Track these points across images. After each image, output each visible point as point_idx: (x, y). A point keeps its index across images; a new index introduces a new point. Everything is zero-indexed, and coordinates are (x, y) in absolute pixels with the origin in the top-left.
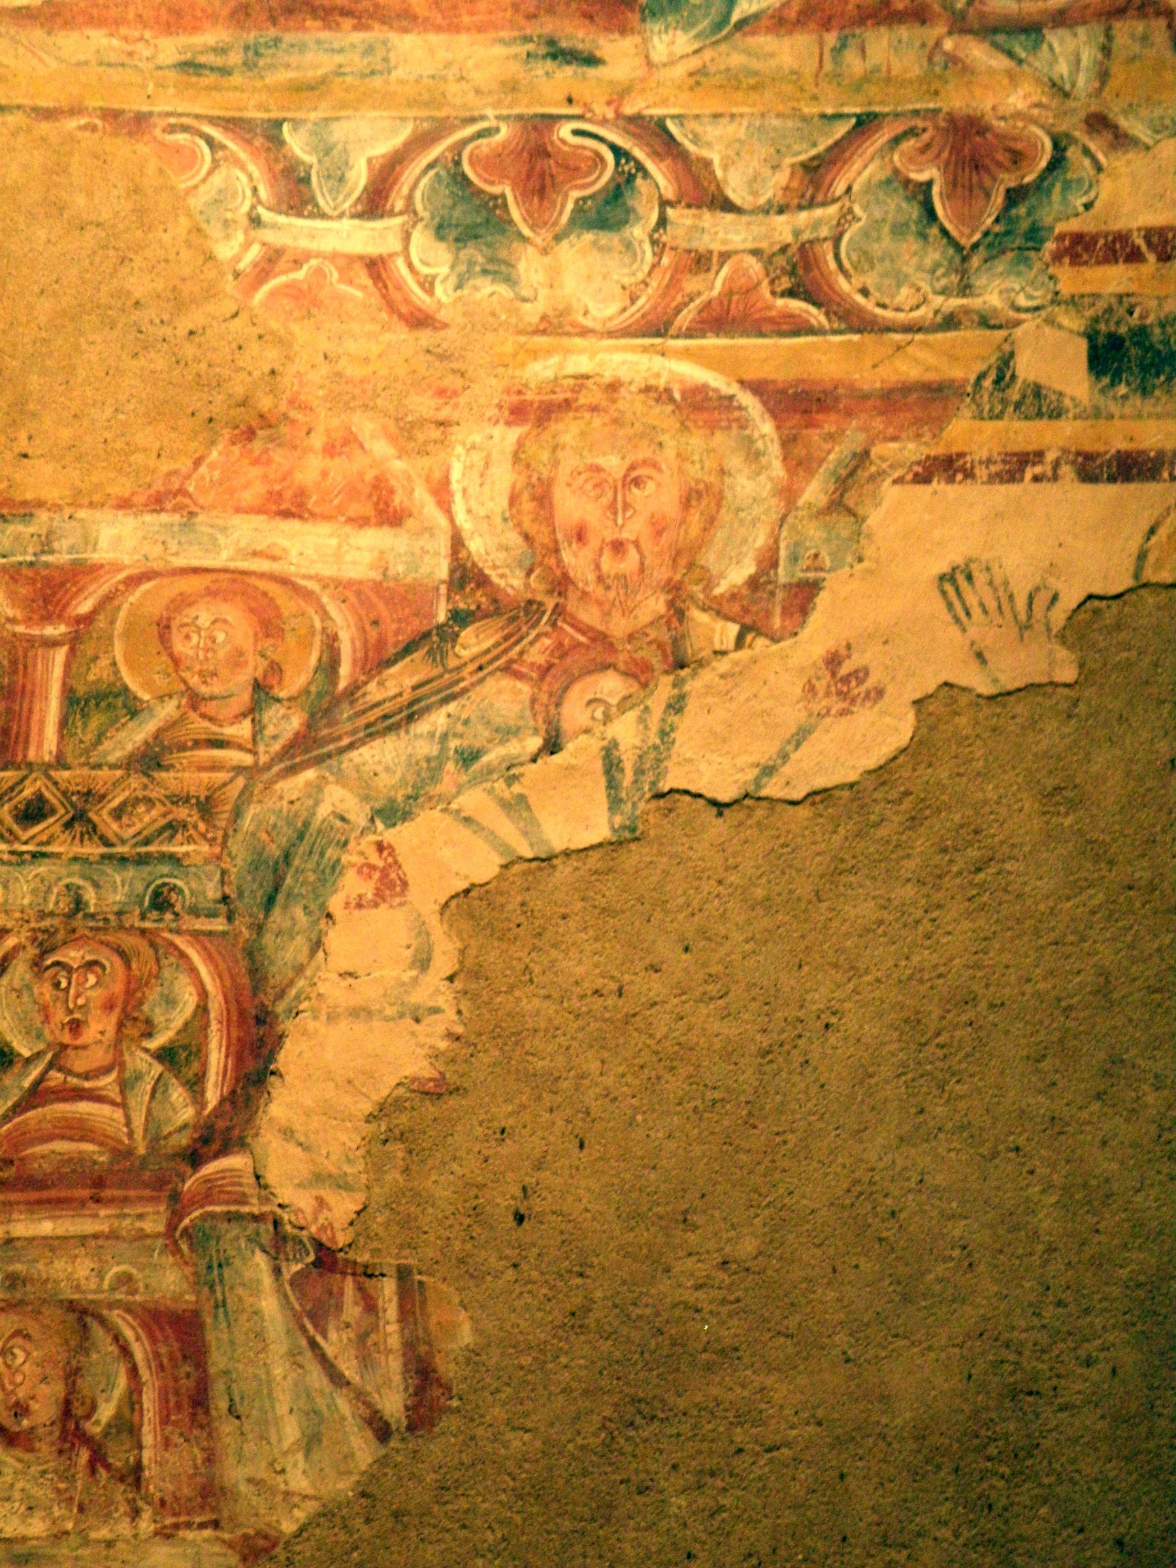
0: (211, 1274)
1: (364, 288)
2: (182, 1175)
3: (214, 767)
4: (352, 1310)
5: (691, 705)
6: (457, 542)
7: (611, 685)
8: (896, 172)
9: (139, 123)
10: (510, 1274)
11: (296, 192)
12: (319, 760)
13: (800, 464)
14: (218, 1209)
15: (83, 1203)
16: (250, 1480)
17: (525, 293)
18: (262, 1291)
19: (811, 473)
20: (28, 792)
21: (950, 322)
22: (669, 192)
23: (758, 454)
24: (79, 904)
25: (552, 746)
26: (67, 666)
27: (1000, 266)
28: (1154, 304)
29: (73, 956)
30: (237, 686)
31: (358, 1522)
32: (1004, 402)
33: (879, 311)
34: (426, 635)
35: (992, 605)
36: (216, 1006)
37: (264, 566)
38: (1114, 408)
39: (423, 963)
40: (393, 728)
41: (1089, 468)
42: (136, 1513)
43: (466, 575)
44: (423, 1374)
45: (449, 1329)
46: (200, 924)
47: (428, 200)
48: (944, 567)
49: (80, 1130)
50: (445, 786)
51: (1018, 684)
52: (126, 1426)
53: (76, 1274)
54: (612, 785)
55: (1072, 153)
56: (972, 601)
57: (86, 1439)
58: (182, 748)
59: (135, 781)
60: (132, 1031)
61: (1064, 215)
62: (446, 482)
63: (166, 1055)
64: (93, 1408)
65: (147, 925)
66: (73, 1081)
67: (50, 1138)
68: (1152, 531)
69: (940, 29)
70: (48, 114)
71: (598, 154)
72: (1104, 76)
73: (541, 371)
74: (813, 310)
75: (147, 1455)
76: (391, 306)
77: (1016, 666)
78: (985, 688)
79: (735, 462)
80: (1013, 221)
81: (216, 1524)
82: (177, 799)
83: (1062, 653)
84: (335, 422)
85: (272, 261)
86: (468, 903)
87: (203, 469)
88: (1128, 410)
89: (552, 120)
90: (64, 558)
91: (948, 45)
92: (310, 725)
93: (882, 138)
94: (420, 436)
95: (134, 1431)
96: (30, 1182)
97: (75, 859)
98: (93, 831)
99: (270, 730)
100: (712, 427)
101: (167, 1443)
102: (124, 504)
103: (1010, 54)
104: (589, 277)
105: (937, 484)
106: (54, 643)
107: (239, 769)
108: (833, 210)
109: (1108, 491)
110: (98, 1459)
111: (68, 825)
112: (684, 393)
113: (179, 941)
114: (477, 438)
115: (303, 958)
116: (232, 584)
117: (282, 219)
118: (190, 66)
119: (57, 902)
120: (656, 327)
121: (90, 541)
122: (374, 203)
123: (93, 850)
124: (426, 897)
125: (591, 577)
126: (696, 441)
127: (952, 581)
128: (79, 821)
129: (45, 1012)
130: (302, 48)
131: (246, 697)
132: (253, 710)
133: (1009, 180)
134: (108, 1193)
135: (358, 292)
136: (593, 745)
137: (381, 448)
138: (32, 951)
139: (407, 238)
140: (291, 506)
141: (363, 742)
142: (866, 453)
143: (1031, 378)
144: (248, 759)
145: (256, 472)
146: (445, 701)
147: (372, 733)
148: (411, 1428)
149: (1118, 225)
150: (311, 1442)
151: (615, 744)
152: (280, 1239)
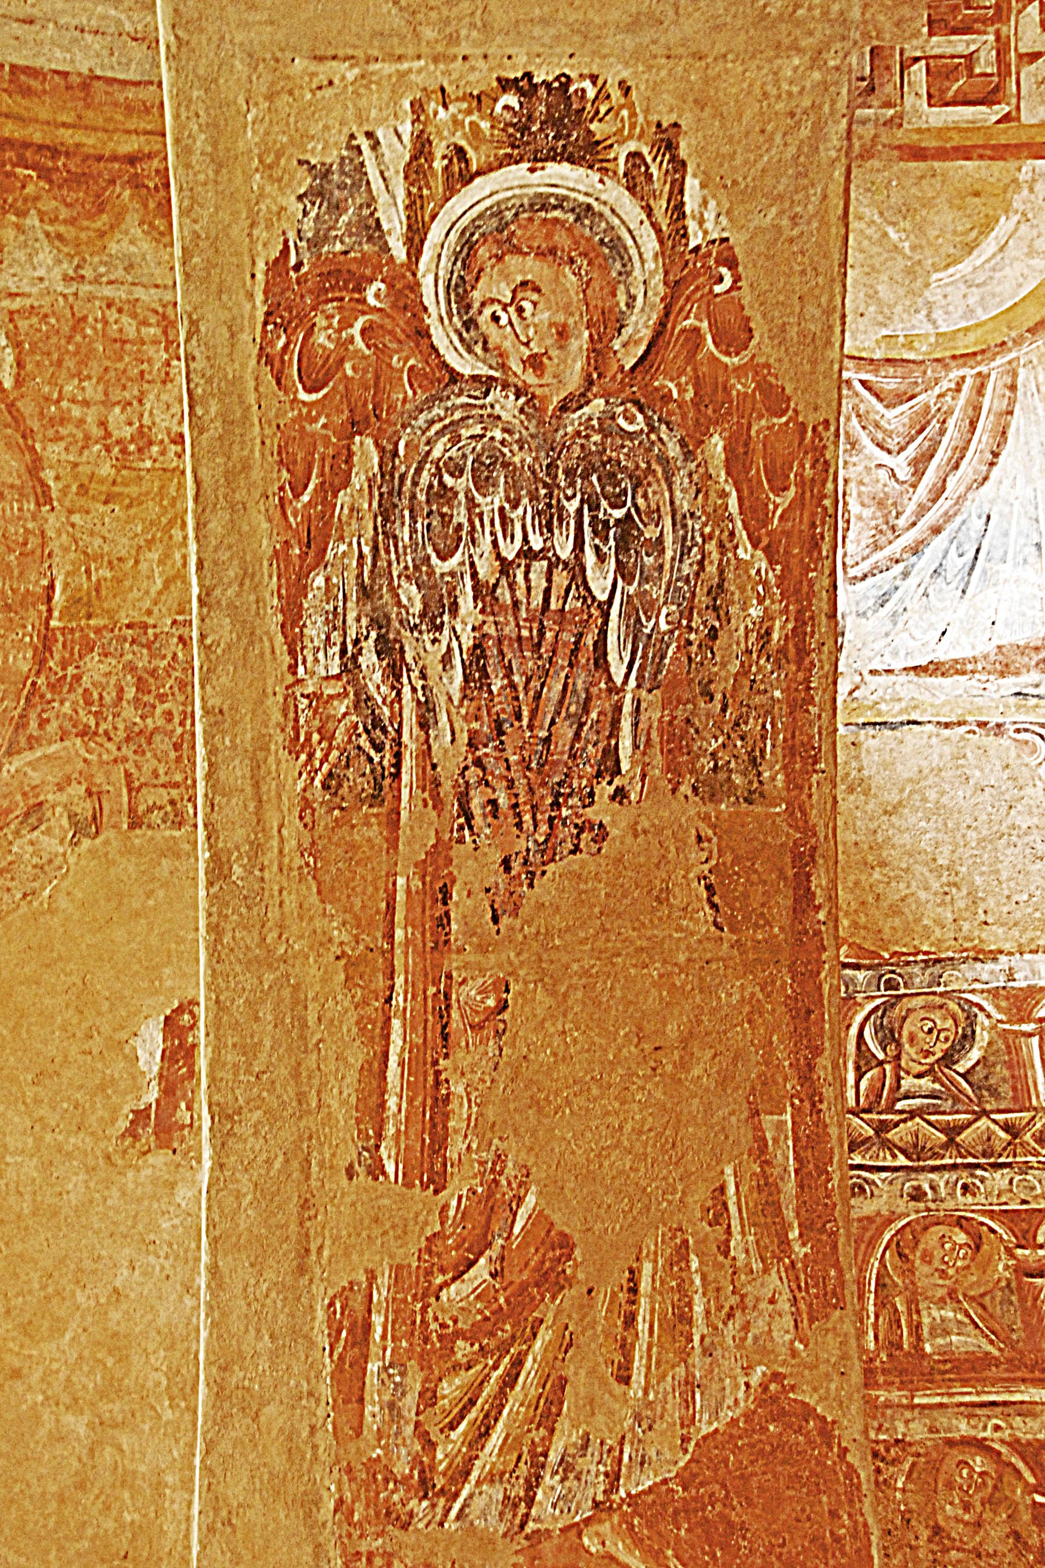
70: (947, 725)
90: (1023, 984)
106: (1031, 1035)
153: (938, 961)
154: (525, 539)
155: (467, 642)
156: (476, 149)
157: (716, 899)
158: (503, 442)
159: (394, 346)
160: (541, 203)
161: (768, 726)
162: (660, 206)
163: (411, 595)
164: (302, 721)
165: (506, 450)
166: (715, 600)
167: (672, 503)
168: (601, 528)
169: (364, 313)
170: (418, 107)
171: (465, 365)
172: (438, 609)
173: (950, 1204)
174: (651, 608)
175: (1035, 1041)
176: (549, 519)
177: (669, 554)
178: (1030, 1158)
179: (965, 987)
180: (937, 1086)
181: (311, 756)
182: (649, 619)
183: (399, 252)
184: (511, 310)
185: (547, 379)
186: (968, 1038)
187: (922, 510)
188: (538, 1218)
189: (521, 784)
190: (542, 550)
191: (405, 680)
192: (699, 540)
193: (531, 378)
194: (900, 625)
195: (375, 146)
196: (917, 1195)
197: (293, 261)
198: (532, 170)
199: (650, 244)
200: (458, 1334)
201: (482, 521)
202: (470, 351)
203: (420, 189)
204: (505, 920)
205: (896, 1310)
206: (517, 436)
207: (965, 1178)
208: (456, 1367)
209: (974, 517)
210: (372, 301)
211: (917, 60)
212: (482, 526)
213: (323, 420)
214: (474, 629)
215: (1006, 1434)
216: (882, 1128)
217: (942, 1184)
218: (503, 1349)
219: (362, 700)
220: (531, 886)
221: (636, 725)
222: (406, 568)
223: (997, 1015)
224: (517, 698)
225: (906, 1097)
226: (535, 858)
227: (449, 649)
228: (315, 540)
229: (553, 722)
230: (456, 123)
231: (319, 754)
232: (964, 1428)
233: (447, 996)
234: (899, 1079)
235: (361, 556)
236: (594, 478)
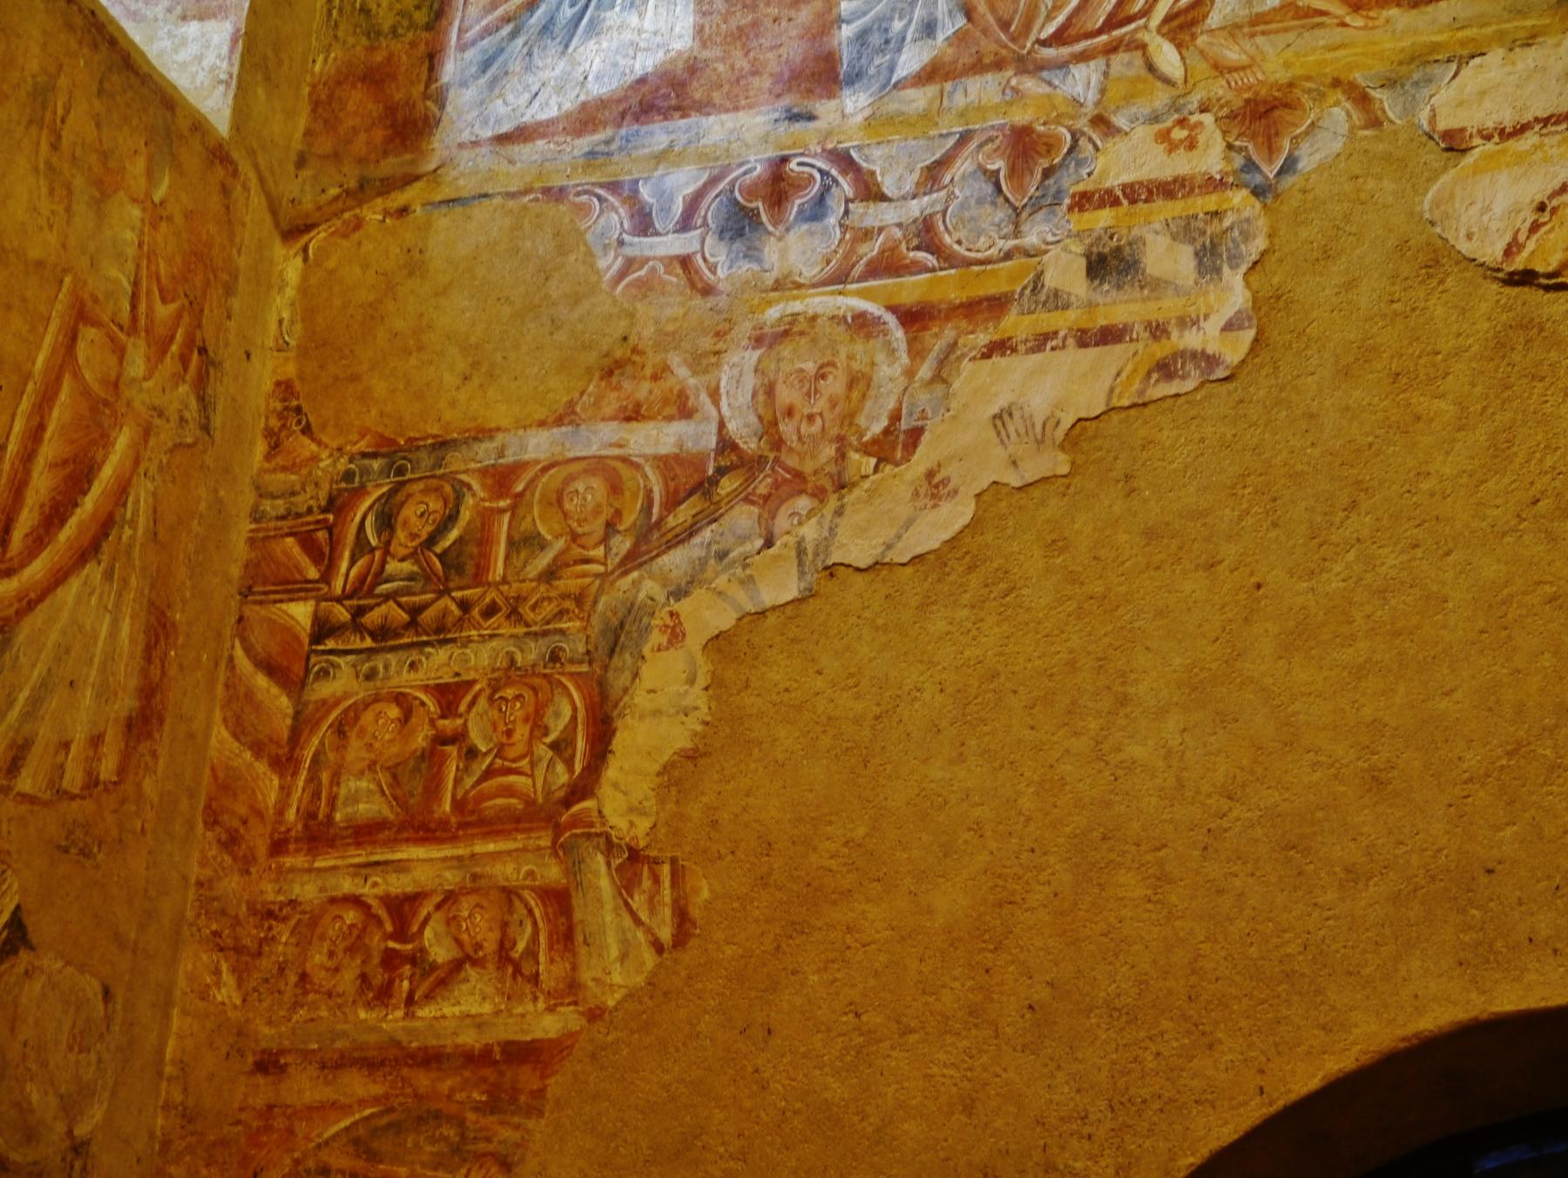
0: (574, 869)
1: (677, 275)
2: (560, 817)
3: (584, 575)
4: (647, 883)
5: (848, 510)
6: (722, 425)
7: (803, 503)
8: (980, 166)
10: (730, 857)
11: (644, 224)
12: (640, 565)
13: (917, 352)
14: (578, 831)
15: (510, 832)
16: (594, 979)
17: (767, 266)
18: (600, 874)
19: (923, 358)
20: (487, 600)
21: (1008, 256)
22: (851, 195)
23: (894, 351)
24: (512, 662)
25: (769, 544)
27: (1040, 216)
28: (1125, 231)
29: (509, 692)
30: (597, 526)
31: (646, 999)
32: (1036, 302)
33: (967, 254)
34: (701, 484)
35: (1022, 431)
36: (581, 715)
38: (1100, 299)
39: (691, 681)
40: (682, 541)
41: (1084, 339)
42: (535, 999)
43: (726, 445)
44: (682, 916)
45: (696, 891)
47: (715, 217)
48: (996, 410)
49: (509, 791)
50: (709, 574)
51: (1036, 478)
52: (531, 952)
53: (506, 872)
54: (801, 564)
55: (1083, 142)
56: (1011, 429)
57: (510, 960)
58: (567, 565)
59: (543, 588)
60: (537, 733)
61: (1071, 182)
62: (718, 387)
63: (555, 746)
64: (515, 944)
65: (547, 671)
66: (507, 764)
68: (1118, 375)
69: (1010, 73)
71: (811, 176)
72: (1103, 91)
73: (773, 313)
74: (930, 257)
75: (541, 968)
76: (693, 285)
77: (1032, 470)
78: (1017, 484)
79: (880, 357)
80: (1047, 188)
81: (575, 1003)
82: (565, 596)
83: (1062, 457)
84: (658, 359)
85: (630, 264)
86: (719, 643)
87: (585, 398)
88: (1108, 300)
89: (785, 160)
91: (1014, 82)
92: (636, 545)
93: (973, 145)
94: (705, 362)
95: (535, 956)
96: (482, 822)
97: (511, 636)
99: (614, 550)
100: (868, 336)
101: (552, 961)
102: (542, 424)
103: (1050, 84)
104: (804, 253)
105: (995, 359)
106: (502, 511)
107: (597, 575)
108: (943, 193)
109: (1092, 352)
110: (517, 971)
112: (853, 318)
113: (564, 680)
114: (735, 359)
115: (628, 683)
116: (597, 465)
117: (636, 239)
118: (592, 154)
119: (501, 662)
120: (840, 278)
121: (523, 448)
122: (685, 224)
123: (521, 630)
124: (694, 642)
125: (795, 438)
126: (859, 347)
127: (1000, 419)
128: (514, 615)
129: (495, 726)
130: (652, 134)
132: (605, 540)
133: (1044, 163)
134: (522, 826)
135: (675, 279)
136: (791, 540)
137: (682, 372)
138: (488, 691)
140: (633, 414)
141: (664, 552)
142: (956, 343)
143: (1053, 285)
145: (613, 395)
146: (710, 523)
147: (670, 546)
148: (675, 946)
149: (1108, 185)
150: (623, 957)
151: (803, 539)
152: (610, 847)
173: (394, 682)
175: (506, 518)
178: (474, 633)
179: (463, 467)
180: (415, 568)
186: (451, 519)
194: (497, 91)
196: (371, 675)
205: (320, 784)
207: (414, 655)
215: (379, 891)
216: (359, 612)
223: (482, 494)
225: (387, 581)
232: (347, 886)
234: (384, 563)
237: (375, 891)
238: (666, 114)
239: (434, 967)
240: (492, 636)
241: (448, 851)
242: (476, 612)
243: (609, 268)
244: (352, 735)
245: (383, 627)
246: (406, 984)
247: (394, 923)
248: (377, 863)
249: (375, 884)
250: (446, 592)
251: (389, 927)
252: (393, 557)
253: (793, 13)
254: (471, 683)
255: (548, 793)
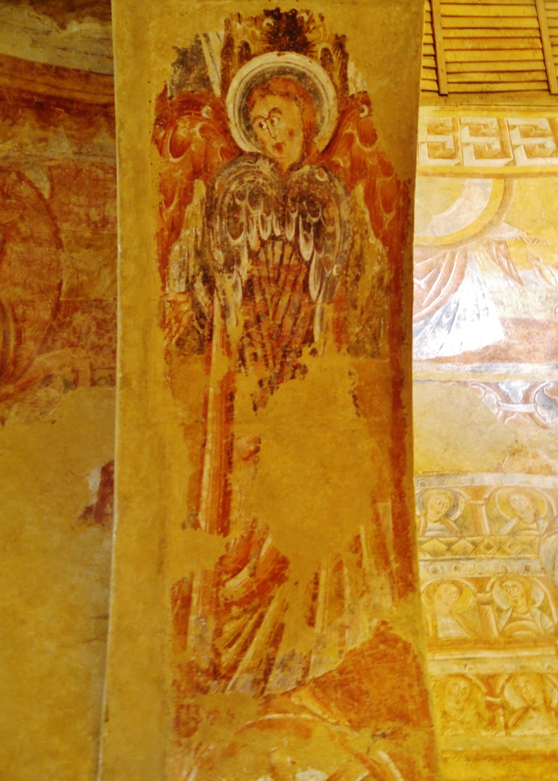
3: (530, 535)
9: (465, 384)
11: (507, 399)
24: (506, 571)
26: (486, 510)
29: (509, 583)
30: (529, 516)
36: (549, 596)
37: (527, 485)
46: (538, 575)
53: (537, 666)
58: (521, 530)
63: (540, 608)
67: (518, 630)
70: (444, 382)
76: (538, 424)
82: (523, 543)
96: (517, 641)
97: (502, 559)
98: (504, 552)
99: (541, 526)
102: (489, 471)
107: (537, 536)
111: (498, 550)
113: (535, 580)
116: (519, 490)
117: (505, 404)
118: (473, 371)
122: (526, 400)
123: (507, 557)
131: (532, 518)
132: (535, 521)
135: (528, 420)
137: (546, 457)
139: (536, 409)
144: (537, 533)
153: (442, 475)
154: (273, 231)
155: (245, 277)
156: (253, 43)
157: (358, 402)
158: (263, 185)
159: (214, 137)
160: (282, 71)
161: (382, 322)
162: (336, 74)
163: (219, 256)
164: (167, 313)
165: (264, 188)
166: (358, 262)
167: (340, 216)
168: (307, 226)
169: (200, 121)
170: (228, 23)
171: (246, 146)
172: (232, 261)
174: (329, 265)
175: (484, 508)
176: (284, 221)
177: (338, 239)
181: (171, 330)
182: (328, 270)
183: (217, 91)
184: (268, 121)
185: (284, 155)
186: (455, 506)
187: (431, 300)
188: (273, 550)
189: (268, 346)
190: (280, 236)
191: (215, 295)
192: (352, 234)
193: (275, 154)
194: (424, 343)
195: (208, 40)
196: (435, 571)
197: (169, 94)
198: (279, 55)
199: (331, 92)
200: (234, 603)
201: (252, 221)
202: (249, 140)
203: (228, 62)
204: (260, 410)
206: (269, 182)
207: (455, 564)
208: (232, 618)
209: (452, 303)
210: (204, 115)
211: (423, 143)
212: (253, 223)
213: (180, 172)
214: (248, 272)
215: (474, 671)
217: (446, 567)
218: (255, 610)
219: (195, 305)
220: (272, 393)
221: (322, 319)
222: (217, 243)
223: (468, 497)
224: (267, 305)
225: (430, 530)
226: (274, 381)
227: (236, 283)
228: (175, 228)
229: (283, 317)
230: (245, 31)
231: (175, 329)
232: (456, 669)
233: (232, 444)
234: (426, 523)
235: (197, 236)
236: (304, 203)
237: (471, 672)
238: (503, 360)
239: (513, 712)
240: (493, 558)
241: (503, 654)
242: (482, 547)
243: (498, 414)
244: (435, 598)
245: (434, 551)
246: (502, 718)
247: (486, 687)
248: (468, 659)
249: (470, 669)
250: (462, 537)
251: (484, 689)
252: (430, 521)
253: (544, 332)
254: (489, 578)
255: (545, 631)
